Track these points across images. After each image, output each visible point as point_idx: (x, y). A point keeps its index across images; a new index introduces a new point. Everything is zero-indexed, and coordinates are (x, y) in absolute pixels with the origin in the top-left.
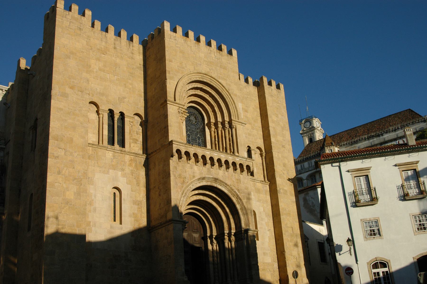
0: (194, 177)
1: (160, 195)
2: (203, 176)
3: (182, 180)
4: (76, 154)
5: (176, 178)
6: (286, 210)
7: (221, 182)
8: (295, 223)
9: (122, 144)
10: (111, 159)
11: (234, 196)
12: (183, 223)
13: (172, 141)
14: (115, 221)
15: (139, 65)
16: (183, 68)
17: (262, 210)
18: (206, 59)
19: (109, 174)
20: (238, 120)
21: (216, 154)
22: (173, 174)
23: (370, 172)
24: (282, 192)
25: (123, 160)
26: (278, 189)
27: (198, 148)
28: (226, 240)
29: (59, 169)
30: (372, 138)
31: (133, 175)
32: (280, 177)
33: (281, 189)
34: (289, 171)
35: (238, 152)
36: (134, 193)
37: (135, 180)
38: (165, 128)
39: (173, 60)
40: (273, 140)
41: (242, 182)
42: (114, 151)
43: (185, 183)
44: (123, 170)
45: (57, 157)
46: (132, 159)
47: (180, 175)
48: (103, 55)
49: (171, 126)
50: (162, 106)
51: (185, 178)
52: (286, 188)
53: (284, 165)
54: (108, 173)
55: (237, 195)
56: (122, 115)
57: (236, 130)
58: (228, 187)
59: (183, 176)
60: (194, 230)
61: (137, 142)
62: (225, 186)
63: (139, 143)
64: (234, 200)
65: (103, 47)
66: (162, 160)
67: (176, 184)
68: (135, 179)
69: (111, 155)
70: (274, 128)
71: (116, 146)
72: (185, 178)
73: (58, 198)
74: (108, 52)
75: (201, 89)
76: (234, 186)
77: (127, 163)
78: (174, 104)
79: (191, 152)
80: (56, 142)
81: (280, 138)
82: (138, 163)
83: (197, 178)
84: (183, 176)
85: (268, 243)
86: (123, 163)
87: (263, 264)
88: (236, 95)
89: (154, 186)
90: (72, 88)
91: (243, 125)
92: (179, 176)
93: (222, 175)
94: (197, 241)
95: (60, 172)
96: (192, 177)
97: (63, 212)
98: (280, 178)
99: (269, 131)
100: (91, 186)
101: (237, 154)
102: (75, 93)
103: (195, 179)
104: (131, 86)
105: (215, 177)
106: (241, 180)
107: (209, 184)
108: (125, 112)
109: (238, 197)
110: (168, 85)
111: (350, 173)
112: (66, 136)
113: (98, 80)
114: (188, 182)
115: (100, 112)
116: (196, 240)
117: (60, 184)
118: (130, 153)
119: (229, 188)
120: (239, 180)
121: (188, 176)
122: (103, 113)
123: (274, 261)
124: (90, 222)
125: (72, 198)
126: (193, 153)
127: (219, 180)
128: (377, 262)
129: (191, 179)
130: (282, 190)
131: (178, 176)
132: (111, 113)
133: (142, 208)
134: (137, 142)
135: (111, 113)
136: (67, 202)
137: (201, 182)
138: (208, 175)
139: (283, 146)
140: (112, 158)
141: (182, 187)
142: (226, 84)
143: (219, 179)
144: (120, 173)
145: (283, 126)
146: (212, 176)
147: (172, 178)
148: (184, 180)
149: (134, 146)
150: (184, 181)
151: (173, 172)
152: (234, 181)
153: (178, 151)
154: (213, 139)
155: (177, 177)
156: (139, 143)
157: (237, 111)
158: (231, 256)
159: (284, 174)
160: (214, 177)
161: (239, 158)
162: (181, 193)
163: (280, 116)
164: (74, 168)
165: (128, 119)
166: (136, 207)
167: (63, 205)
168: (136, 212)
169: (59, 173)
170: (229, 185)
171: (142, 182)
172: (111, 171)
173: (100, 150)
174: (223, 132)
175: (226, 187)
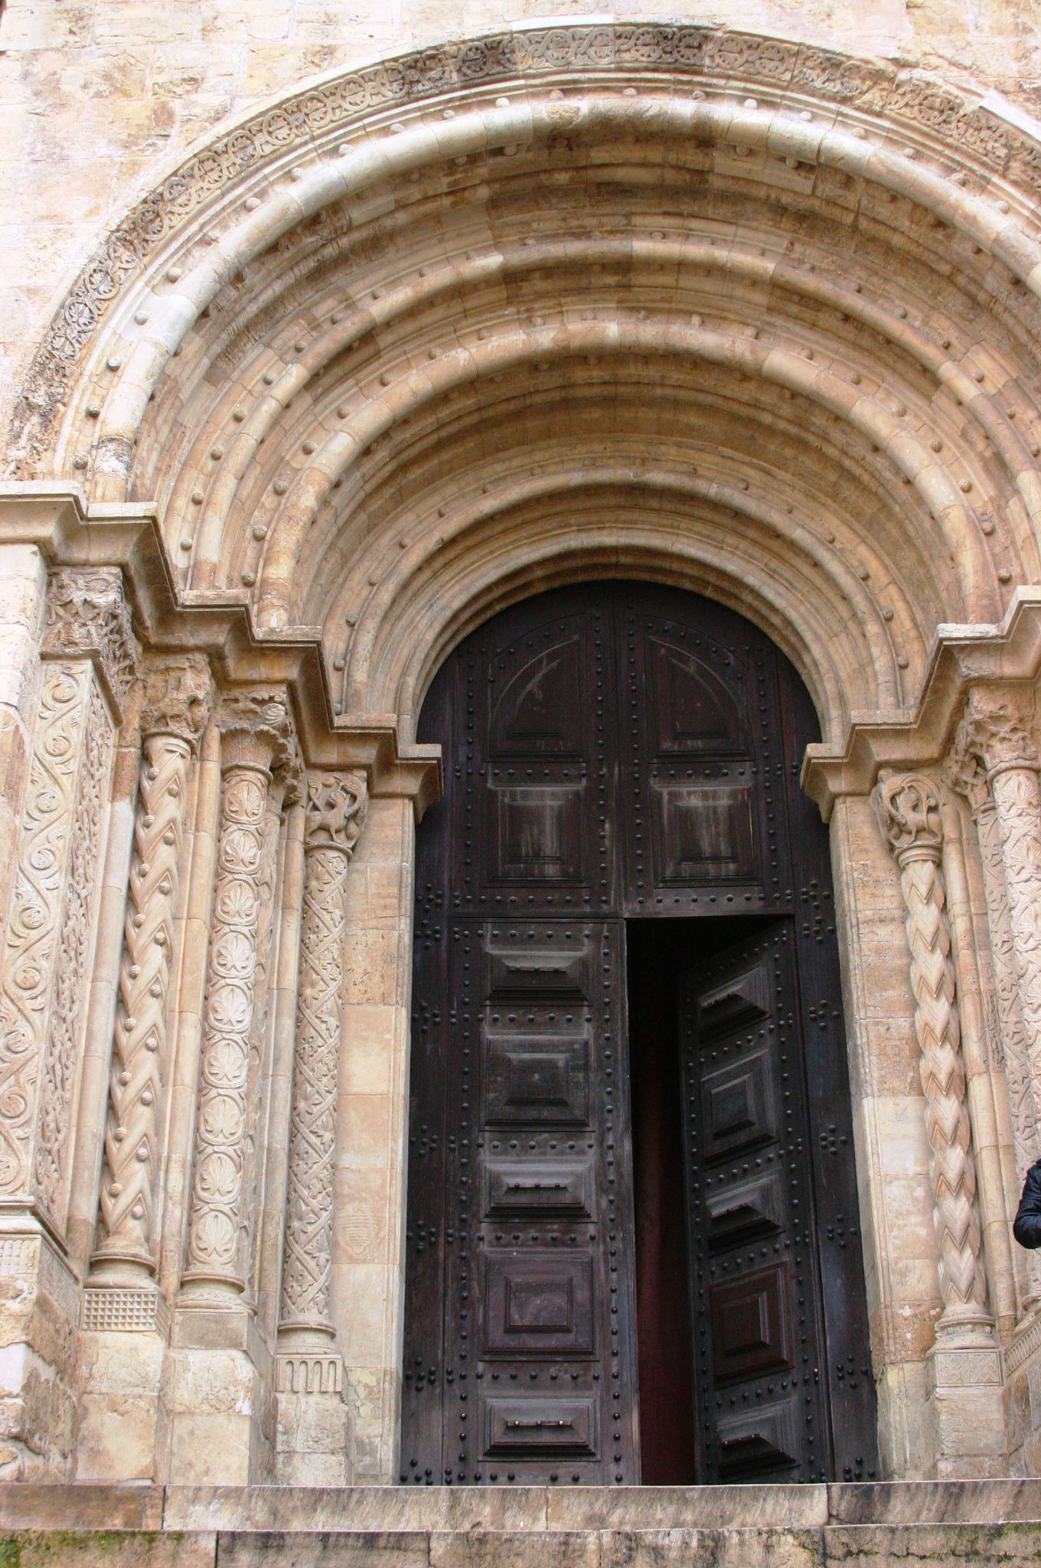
0: (328, 52)
2: (475, 27)
3: (140, 108)
11: (982, 186)
12: (48, 529)
22: (26, 75)
28: (998, 746)
43: (173, 132)
47: (117, 75)
59: (161, 70)
60: (677, 737)
62: (835, 87)
72: (193, 80)
76: (968, 64)
84: (161, 70)
92: (107, 77)
94: (716, 858)
96: (293, 60)
107: (583, 106)
116: (706, 848)
127: (722, 46)
131: (85, 87)
137: (464, 106)
138: (552, 12)
141: (132, 168)
143: (719, 34)
146: (605, 9)
148: (176, 105)
150: (163, 116)
160: (640, 19)
170: (881, 65)
175: (845, 100)
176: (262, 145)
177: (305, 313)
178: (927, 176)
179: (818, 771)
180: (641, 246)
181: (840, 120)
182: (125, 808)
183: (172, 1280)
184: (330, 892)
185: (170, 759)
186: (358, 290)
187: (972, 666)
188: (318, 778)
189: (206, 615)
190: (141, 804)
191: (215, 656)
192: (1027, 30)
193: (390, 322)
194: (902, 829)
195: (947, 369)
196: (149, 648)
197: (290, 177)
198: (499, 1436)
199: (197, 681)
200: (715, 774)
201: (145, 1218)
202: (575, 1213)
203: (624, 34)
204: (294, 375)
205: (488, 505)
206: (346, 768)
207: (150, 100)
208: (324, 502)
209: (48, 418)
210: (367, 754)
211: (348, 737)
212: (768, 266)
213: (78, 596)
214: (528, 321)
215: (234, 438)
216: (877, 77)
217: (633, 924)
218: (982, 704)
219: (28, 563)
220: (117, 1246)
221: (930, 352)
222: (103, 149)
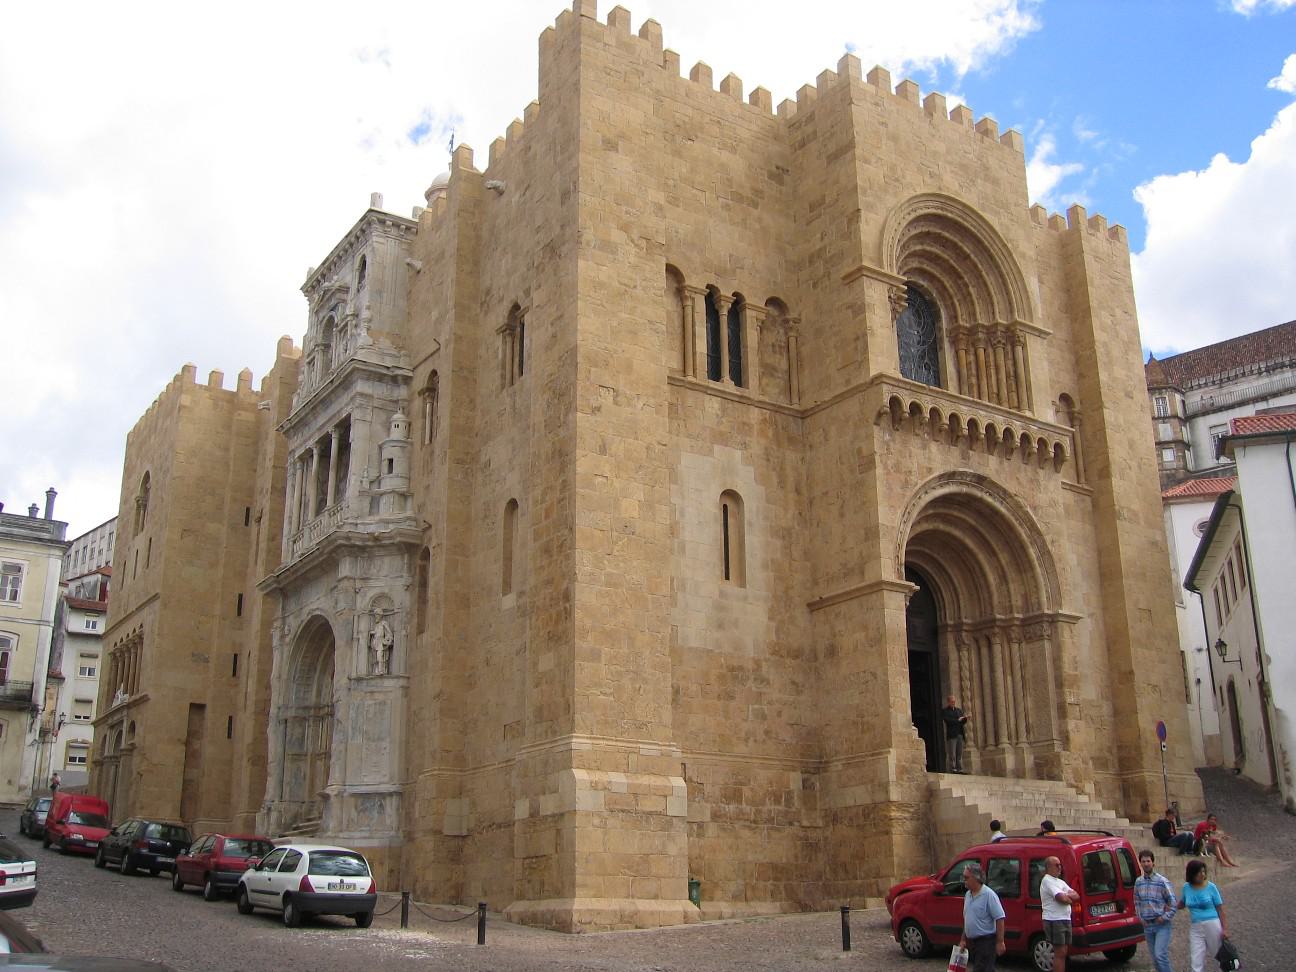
0: (930, 470)
1: (842, 515)
2: (950, 468)
3: (902, 477)
5: (888, 473)
9: (738, 378)
10: (718, 415)
12: (907, 591)
13: (881, 376)
14: (727, 578)
15: (774, 169)
16: (897, 180)
17: (1075, 562)
18: (949, 158)
19: (713, 457)
20: (1032, 321)
24: (1126, 515)
25: (745, 420)
26: (1117, 508)
29: (603, 440)
30: (1279, 370)
31: (768, 460)
35: (1030, 408)
36: (773, 507)
37: (774, 473)
38: (857, 339)
39: (873, 160)
40: (1103, 376)
42: (722, 395)
44: (745, 446)
45: (597, 409)
46: (765, 419)
48: (690, 142)
49: (873, 334)
50: (846, 282)
51: (910, 472)
52: (1135, 506)
53: (1131, 445)
54: (711, 452)
55: (1030, 520)
56: (738, 302)
57: (1024, 346)
61: (776, 374)
63: (779, 378)
64: (1023, 533)
65: (687, 119)
66: (850, 423)
67: (890, 489)
68: (774, 469)
69: (716, 406)
70: (1105, 344)
71: (727, 384)
74: (699, 135)
75: (938, 239)
77: (755, 426)
78: (880, 278)
79: (926, 405)
80: (593, 369)
81: (1120, 372)
82: (780, 427)
83: (936, 474)
86: (747, 428)
88: (1023, 256)
89: (824, 491)
90: (625, 228)
91: (1042, 335)
95: (605, 450)
96: (925, 470)
99: (1095, 352)
101: (1028, 414)
102: (632, 241)
103: (931, 477)
104: (757, 226)
105: (980, 472)
107: (965, 489)
108: (745, 294)
109: (1033, 527)
110: (863, 226)
112: (615, 355)
113: (678, 206)
114: (917, 484)
115: (687, 293)
117: (605, 480)
118: (761, 405)
119: (1012, 504)
120: (1034, 481)
121: (915, 468)
125: (635, 514)
126: (931, 406)
130: (1125, 511)
132: (712, 297)
133: (793, 548)
134: (776, 374)
135: (712, 297)
136: (626, 528)
139: (1129, 395)
140: (719, 412)
141: (904, 496)
142: (1001, 225)
144: (738, 454)
145: (1126, 339)
147: (879, 471)
149: (767, 385)
150: (906, 481)
151: (881, 455)
153: (895, 402)
154: (964, 371)
156: (779, 378)
157: (1028, 298)
158: (1009, 678)
159: (1130, 468)
162: (900, 512)
163: (1118, 312)
164: (637, 439)
165: (754, 313)
166: (779, 543)
167: (615, 534)
168: (778, 555)
171: (792, 479)
172: (717, 448)
173: (690, 392)
174: (990, 350)
179: (947, 625)
180: (956, 513)
181: (1002, 503)
187: (998, 623)
194: (964, 643)
195: (1001, 556)
203: (974, 475)
212: (973, 523)
216: (1011, 497)
218: (997, 630)
221: (997, 549)
222: (899, 490)
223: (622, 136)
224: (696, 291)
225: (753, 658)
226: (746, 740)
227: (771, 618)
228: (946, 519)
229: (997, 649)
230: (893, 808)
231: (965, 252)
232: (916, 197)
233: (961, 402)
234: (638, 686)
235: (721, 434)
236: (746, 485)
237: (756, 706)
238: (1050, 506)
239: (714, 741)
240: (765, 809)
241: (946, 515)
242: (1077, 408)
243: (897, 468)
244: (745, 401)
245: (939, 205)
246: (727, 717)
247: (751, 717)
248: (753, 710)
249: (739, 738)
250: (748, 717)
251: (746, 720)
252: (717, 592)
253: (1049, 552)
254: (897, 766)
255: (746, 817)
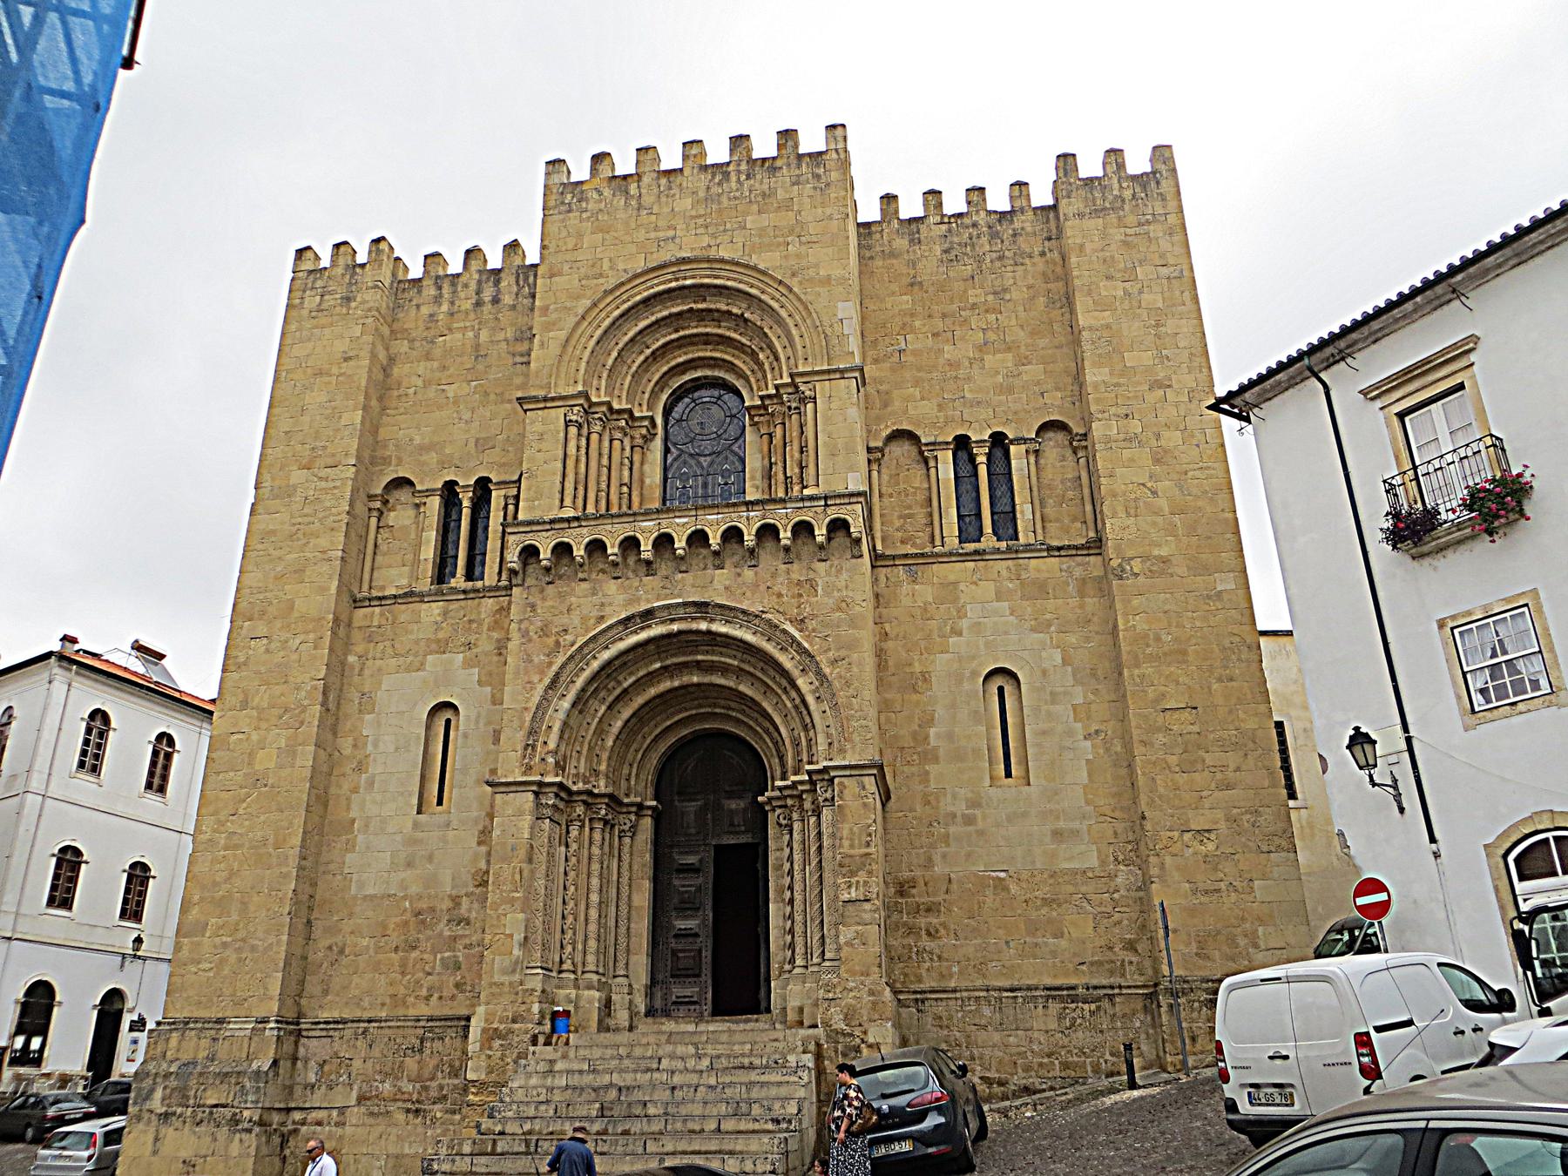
0: (602, 617)
2: (644, 607)
3: (551, 641)
4: (298, 642)
6: (1158, 639)
7: (729, 613)
8: (1215, 686)
19: (424, 670)
21: (685, 520)
23: (1472, 364)
27: (606, 521)
32: (1132, 512)
33: (1132, 559)
34: (1190, 474)
39: (566, 267)
41: (820, 590)
55: (793, 637)
58: (757, 621)
69: (437, 611)
73: (232, 774)
78: (549, 405)
85: (1085, 787)
86: (475, 625)
87: (1052, 876)
93: (727, 583)
96: (592, 621)
97: (241, 811)
98: (1128, 515)
100: (368, 717)
103: (604, 626)
106: (820, 582)
107: (675, 627)
111: (1379, 404)
121: (575, 619)
122: (424, 500)
123: (1116, 860)
124: (353, 821)
128: (1547, 840)
129: (587, 631)
137: (642, 629)
139: (1157, 385)
141: (550, 664)
146: (679, 597)
150: (558, 643)
152: (784, 592)
155: (535, 637)
159: (1154, 493)
161: (788, 505)
165: (503, 492)
169: (245, 705)
176: (586, 651)
177: (605, 687)
178: (769, 647)
180: (700, 657)
182: (563, 849)
183: (579, 973)
184: (626, 849)
185: (574, 832)
186: (621, 678)
188: (621, 816)
189: (579, 793)
190: (567, 846)
191: (584, 802)
192: (800, 595)
193: (630, 686)
196: (567, 802)
197: (594, 657)
198: (674, 998)
199: (580, 810)
200: (740, 797)
201: (573, 959)
202: (696, 935)
204: (603, 708)
205: (668, 723)
206: (630, 813)
207: (554, 638)
208: (615, 742)
209: (534, 747)
210: (634, 809)
211: (628, 805)
213: (544, 801)
214: (672, 677)
215: (587, 731)
216: (757, 616)
217: (716, 846)
219: (531, 796)
220: (565, 967)
223: (320, 373)
224: (429, 492)
225: (450, 896)
226: (427, 998)
227: (479, 843)
228: (699, 666)
229: (797, 826)
230: (473, 1090)
231: (736, 315)
232: (623, 284)
233: (641, 518)
234: (244, 956)
235: (438, 641)
236: (465, 691)
237: (447, 954)
238: (839, 609)
239: (383, 1005)
240: (434, 1084)
241: (698, 662)
242: (1077, 429)
243: (544, 631)
244: (472, 595)
245: (669, 276)
246: (403, 973)
247: (438, 968)
248: (442, 959)
249: (417, 997)
250: (433, 968)
251: (429, 974)
252: (410, 824)
253: (825, 676)
254: (484, 1031)
255: (406, 1096)
